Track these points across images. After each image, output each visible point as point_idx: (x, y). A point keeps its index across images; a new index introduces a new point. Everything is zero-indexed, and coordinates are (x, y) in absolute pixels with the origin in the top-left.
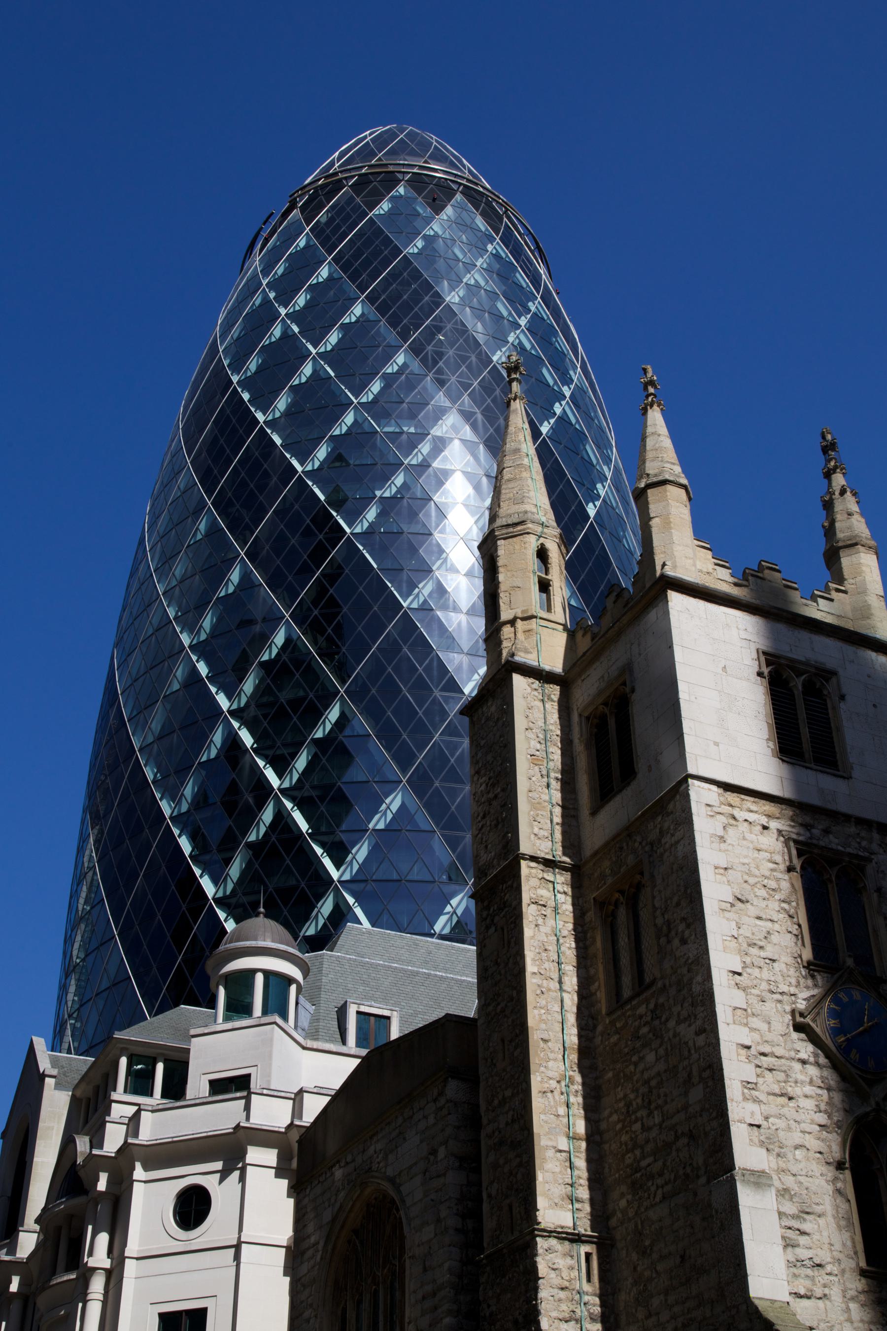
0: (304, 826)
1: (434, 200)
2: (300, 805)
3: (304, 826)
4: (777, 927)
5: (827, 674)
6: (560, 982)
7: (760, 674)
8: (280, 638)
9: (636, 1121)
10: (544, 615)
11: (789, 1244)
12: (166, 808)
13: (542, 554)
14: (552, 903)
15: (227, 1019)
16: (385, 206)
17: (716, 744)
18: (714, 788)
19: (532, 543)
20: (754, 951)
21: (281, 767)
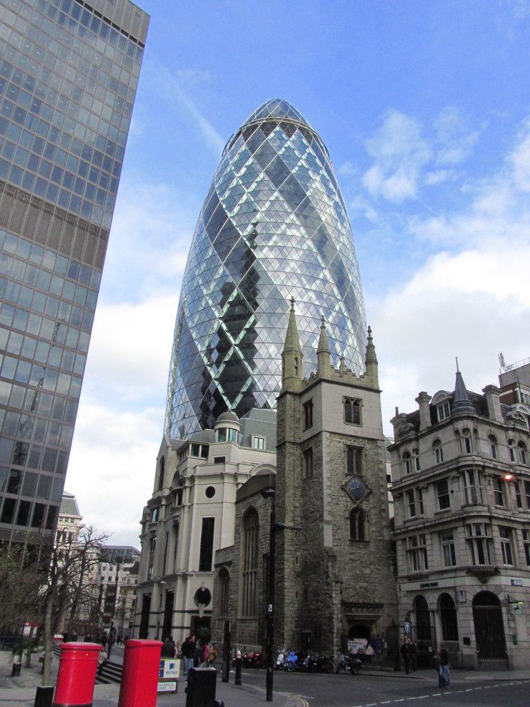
0: (242, 356)
2: (241, 349)
3: (242, 356)
5: (360, 400)
8: (235, 293)
11: (334, 535)
12: (199, 347)
13: (296, 359)
15: (219, 441)
16: (272, 135)
19: (294, 357)
21: (235, 335)
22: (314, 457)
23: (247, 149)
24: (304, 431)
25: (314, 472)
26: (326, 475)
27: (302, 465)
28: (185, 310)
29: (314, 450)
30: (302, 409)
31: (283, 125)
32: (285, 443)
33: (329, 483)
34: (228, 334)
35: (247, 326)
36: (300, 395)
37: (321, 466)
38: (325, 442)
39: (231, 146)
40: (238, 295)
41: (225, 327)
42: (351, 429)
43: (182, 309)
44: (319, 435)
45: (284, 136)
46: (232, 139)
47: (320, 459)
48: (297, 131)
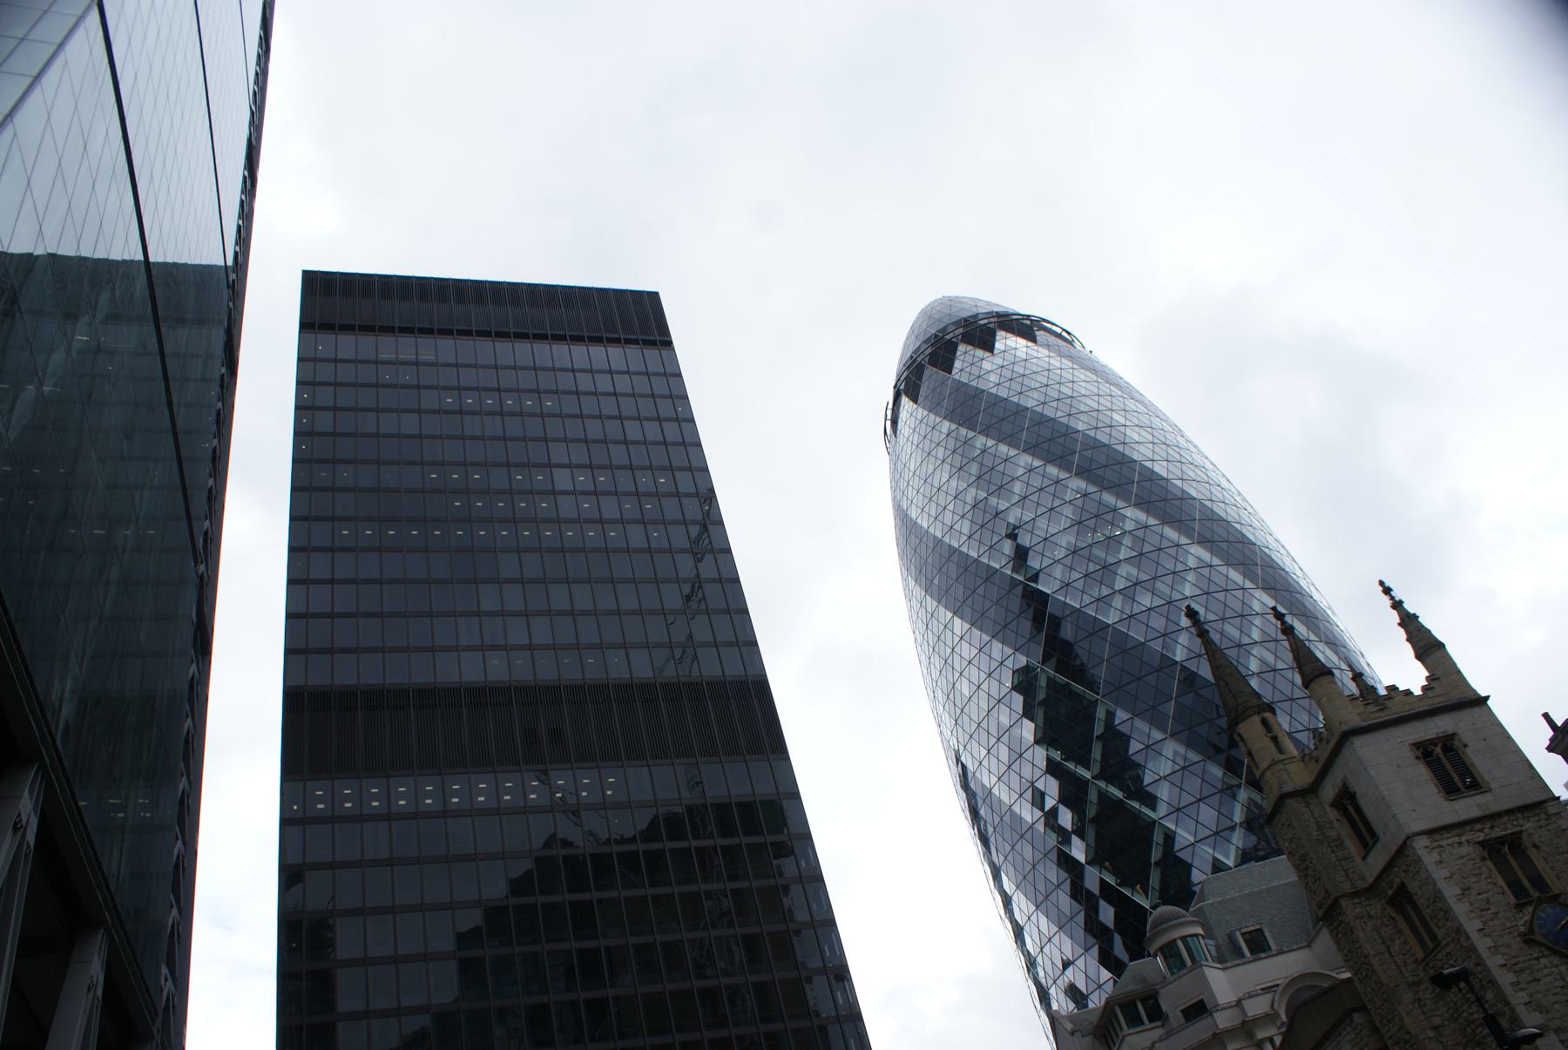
0: (1119, 794)
1: (985, 343)
2: (1110, 781)
3: (1119, 794)
4: (1490, 893)
6: (1390, 953)
7: (1418, 758)
8: (1043, 682)
9: (1463, 1011)
10: (1282, 757)
14: (1365, 914)
16: (958, 364)
17: (1414, 810)
18: (1424, 836)
19: (1256, 719)
20: (1485, 913)
22: (1421, 902)
23: (926, 413)
24: (1364, 858)
25: (1440, 933)
26: (1471, 926)
27: (1400, 932)
28: (963, 759)
29: (1413, 886)
30: (1333, 815)
31: (969, 339)
32: (1336, 901)
33: (1488, 942)
34: (1071, 766)
35: (1099, 729)
36: (1313, 789)
37: (1447, 913)
38: (1429, 860)
39: (895, 422)
40: (1049, 680)
41: (1057, 755)
42: (1466, 807)
43: (958, 760)
44: (1403, 850)
45: (980, 353)
46: (889, 412)
47: (1438, 897)
48: (1000, 334)
